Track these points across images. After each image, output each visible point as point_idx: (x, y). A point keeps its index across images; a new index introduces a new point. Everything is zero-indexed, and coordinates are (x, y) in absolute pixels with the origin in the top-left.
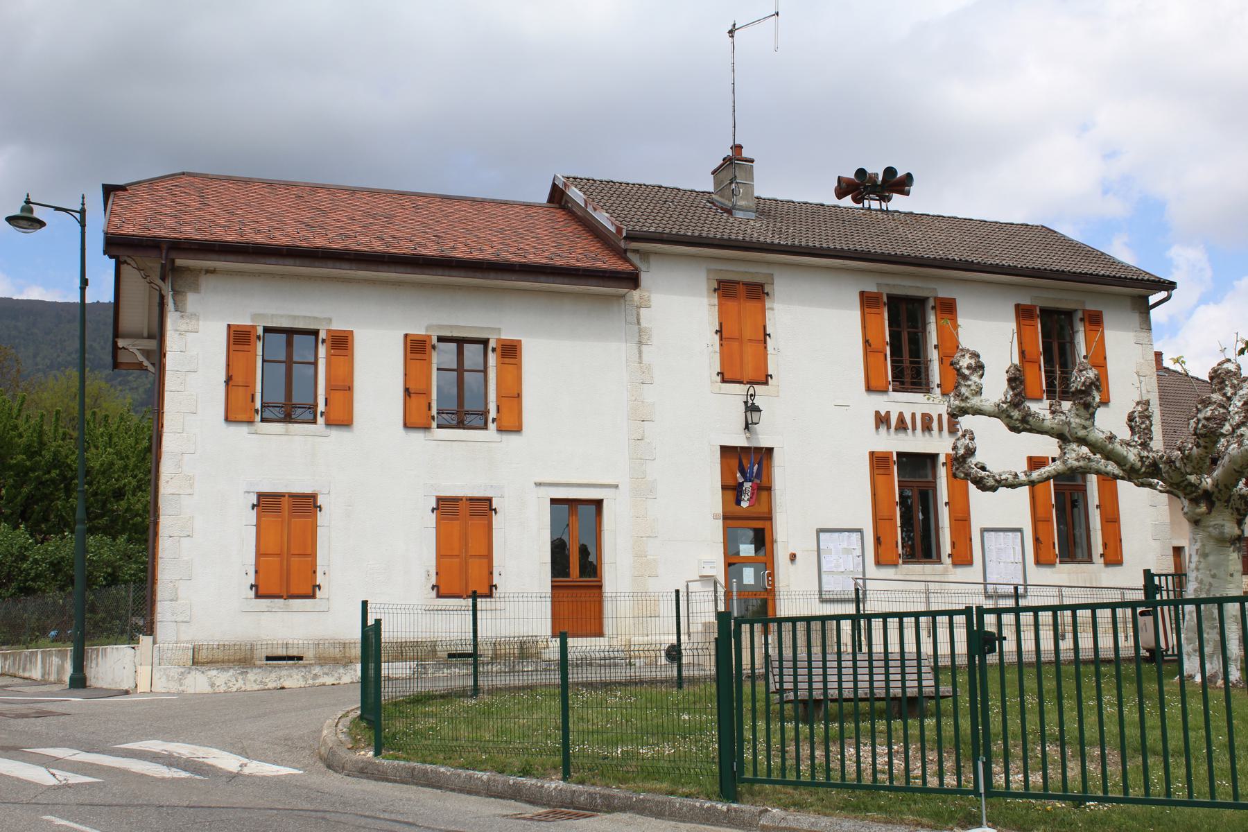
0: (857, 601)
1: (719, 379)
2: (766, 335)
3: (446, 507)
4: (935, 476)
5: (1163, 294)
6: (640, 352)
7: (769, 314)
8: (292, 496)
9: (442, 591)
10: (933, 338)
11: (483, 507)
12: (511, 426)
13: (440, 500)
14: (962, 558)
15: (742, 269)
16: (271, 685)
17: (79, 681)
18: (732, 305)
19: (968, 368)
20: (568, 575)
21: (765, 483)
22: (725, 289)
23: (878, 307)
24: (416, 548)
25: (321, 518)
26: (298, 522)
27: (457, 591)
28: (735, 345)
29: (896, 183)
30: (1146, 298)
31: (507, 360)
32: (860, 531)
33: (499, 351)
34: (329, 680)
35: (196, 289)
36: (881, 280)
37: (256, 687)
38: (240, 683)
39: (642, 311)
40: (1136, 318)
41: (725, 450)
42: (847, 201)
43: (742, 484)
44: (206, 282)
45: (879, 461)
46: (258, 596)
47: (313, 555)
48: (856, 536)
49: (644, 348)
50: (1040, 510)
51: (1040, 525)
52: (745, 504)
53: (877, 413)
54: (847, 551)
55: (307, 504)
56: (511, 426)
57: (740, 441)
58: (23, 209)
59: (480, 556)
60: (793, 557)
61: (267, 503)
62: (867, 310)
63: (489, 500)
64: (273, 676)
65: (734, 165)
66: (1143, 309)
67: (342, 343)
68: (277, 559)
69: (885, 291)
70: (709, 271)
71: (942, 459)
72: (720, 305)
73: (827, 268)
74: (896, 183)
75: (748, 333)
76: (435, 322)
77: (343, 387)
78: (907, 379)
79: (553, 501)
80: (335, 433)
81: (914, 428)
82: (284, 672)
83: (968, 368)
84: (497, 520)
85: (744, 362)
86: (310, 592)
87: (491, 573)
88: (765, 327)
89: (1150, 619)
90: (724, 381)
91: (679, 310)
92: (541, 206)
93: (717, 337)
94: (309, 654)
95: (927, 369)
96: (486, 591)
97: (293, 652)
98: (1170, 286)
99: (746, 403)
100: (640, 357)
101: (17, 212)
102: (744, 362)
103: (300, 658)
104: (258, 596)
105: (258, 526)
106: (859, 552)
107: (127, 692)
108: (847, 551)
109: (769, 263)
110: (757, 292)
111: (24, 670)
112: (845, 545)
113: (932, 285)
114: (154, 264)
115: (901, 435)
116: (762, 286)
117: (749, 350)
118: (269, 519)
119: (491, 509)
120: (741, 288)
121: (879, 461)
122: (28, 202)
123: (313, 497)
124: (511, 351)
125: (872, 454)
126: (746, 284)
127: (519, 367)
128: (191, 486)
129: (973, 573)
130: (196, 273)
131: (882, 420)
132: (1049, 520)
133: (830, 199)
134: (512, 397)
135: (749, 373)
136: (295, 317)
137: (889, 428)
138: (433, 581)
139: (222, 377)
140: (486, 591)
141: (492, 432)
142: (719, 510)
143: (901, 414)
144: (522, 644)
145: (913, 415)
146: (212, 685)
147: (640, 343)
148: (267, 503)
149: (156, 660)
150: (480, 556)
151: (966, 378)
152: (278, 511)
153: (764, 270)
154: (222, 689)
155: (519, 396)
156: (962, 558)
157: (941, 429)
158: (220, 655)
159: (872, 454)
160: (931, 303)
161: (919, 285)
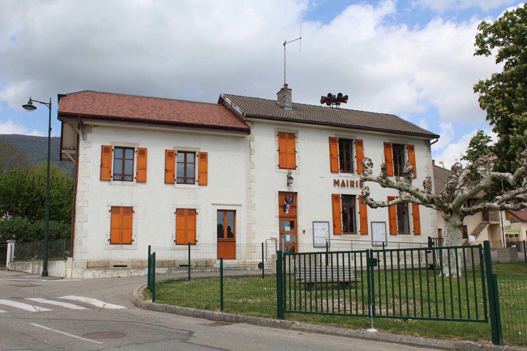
0: (384, 246)
1: (278, 167)
2: (295, 152)
3: (180, 212)
4: (355, 203)
5: (435, 140)
6: (250, 157)
7: (296, 144)
8: (124, 207)
9: (178, 243)
10: (355, 154)
11: (193, 212)
12: (204, 183)
13: (177, 209)
14: (364, 232)
15: (287, 128)
16: (115, 276)
17: (45, 274)
18: (283, 141)
19: (367, 164)
20: (223, 237)
21: (294, 205)
22: (281, 135)
23: (335, 142)
24: (168, 227)
25: (134, 216)
26: (126, 217)
27: (183, 243)
28: (284, 155)
29: (342, 99)
30: (429, 141)
31: (202, 160)
32: (328, 222)
33: (199, 156)
34: (136, 274)
35: (90, 132)
37: (110, 277)
38: (104, 275)
40: (426, 148)
41: (280, 193)
42: (325, 105)
43: (286, 205)
44: (94, 130)
45: (335, 197)
46: (111, 243)
48: (326, 224)
49: (252, 156)
50: (392, 215)
51: (392, 220)
52: (287, 212)
53: (335, 180)
54: (323, 229)
55: (129, 211)
56: (204, 183)
57: (285, 189)
58: (29, 103)
59: (192, 230)
60: (304, 231)
61: (114, 210)
63: (195, 210)
64: (116, 272)
65: (285, 91)
66: (429, 145)
67: (143, 152)
68: (118, 230)
69: (338, 137)
70: (275, 129)
71: (357, 197)
73: (317, 128)
74: (342, 99)
75: (289, 151)
76: (177, 146)
77: (143, 169)
79: (218, 210)
80: (140, 185)
81: (348, 186)
82: (120, 271)
83: (367, 164)
84: (198, 217)
85: (287, 161)
86: (130, 242)
90: (280, 168)
91: (264, 142)
92: (215, 105)
93: (278, 152)
94: (129, 265)
95: (352, 165)
96: (193, 242)
97: (124, 264)
98: (437, 137)
99: (288, 176)
100: (250, 159)
101: (27, 104)
102: (287, 161)
103: (126, 266)
104: (111, 243)
105: (111, 218)
106: (327, 230)
107: (63, 278)
108: (323, 229)
109: (297, 126)
110: (293, 136)
111: (26, 269)
112: (322, 227)
113: (354, 135)
114: (76, 123)
115: (343, 188)
116: (294, 134)
117: (289, 157)
120: (287, 135)
121: (335, 197)
122: (30, 100)
123: (131, 208)
124: (204, 156)
125: (333, 195)
126: (288, 134)
127: (206, 162)
128: (87, 203)
129: (368, 238)
130: (90, 126)
131: (336, 183)
132: (395, 219)
133: (319, 104)
134: (204, 173)
135: (289, 166)
136: (126, 143)
137: (339, 185)
138: (175, 239)
139: (99, 164)
140: (193, 242)
141: (196, 185)
142: (278, 214)
143: (343, 181)
144: (206, 262)
145: (347, 181)
146: (94, 276)
147: (250, 154)
148: (114, 210)
149: (73, 267)
150: (192, 230)
151: (366, 168)
152: (119, 213)
154: (98, 277)
155: (206, 172)
156: (364, 232)
157: (357, 186)
158: (97, 265)
159: (333, 195)
160: (354, 141)
161: (350, 135)
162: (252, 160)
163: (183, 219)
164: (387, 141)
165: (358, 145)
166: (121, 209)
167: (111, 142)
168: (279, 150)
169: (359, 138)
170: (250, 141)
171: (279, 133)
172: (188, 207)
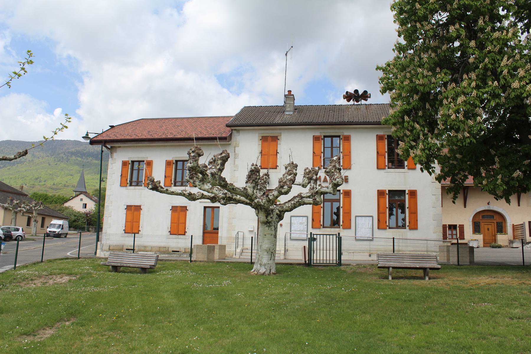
2: (277, 153)
6: (235, 161)
8: (135, 206)
13: (172, 207)
15: (270, 132)
18: (266, 144)
22: (264, 139)
24: (165, 220)
25: (142, 212)
27: (175, 233)
28: (266, 157)
35: (116, 152)
36: (321, 131)
44: (118, 150)
47: (139, 222)
48: (305, 219)
50: (381, 210)
51: (381, 215)
54: (301, 223)
55: (138, 208)
61: (129, 208)
63: (186, 207)
65: (289, 96)
67: (149, 164)
69: (323, 134)
72: (262, 144)
78: (396, 163)
84: (188, 213)
89: (245, 247)
100: (235, 162)
101: (85, 135)
106: (306, 224)
110: (275, 139)
112: (300, 221)
113: (341, 131)
116: (277, 137)
118: (129, 212)
123: (140, 206)
132: (385, 213)
133: (344, 102)
136: (139, 158)
153: (279, 131)
156: (348, 227)
158: (115, 248)
161: (337, 131)
162: (236, 163)
163: (176, 214)
164: (381, 133)
165: (344, 140)
166: (178, 208)
167: (129, 158)
168: (261, 153)
169: (346, 133)
170: (235, 147)
171: (262, 137)
172: (181, 205)
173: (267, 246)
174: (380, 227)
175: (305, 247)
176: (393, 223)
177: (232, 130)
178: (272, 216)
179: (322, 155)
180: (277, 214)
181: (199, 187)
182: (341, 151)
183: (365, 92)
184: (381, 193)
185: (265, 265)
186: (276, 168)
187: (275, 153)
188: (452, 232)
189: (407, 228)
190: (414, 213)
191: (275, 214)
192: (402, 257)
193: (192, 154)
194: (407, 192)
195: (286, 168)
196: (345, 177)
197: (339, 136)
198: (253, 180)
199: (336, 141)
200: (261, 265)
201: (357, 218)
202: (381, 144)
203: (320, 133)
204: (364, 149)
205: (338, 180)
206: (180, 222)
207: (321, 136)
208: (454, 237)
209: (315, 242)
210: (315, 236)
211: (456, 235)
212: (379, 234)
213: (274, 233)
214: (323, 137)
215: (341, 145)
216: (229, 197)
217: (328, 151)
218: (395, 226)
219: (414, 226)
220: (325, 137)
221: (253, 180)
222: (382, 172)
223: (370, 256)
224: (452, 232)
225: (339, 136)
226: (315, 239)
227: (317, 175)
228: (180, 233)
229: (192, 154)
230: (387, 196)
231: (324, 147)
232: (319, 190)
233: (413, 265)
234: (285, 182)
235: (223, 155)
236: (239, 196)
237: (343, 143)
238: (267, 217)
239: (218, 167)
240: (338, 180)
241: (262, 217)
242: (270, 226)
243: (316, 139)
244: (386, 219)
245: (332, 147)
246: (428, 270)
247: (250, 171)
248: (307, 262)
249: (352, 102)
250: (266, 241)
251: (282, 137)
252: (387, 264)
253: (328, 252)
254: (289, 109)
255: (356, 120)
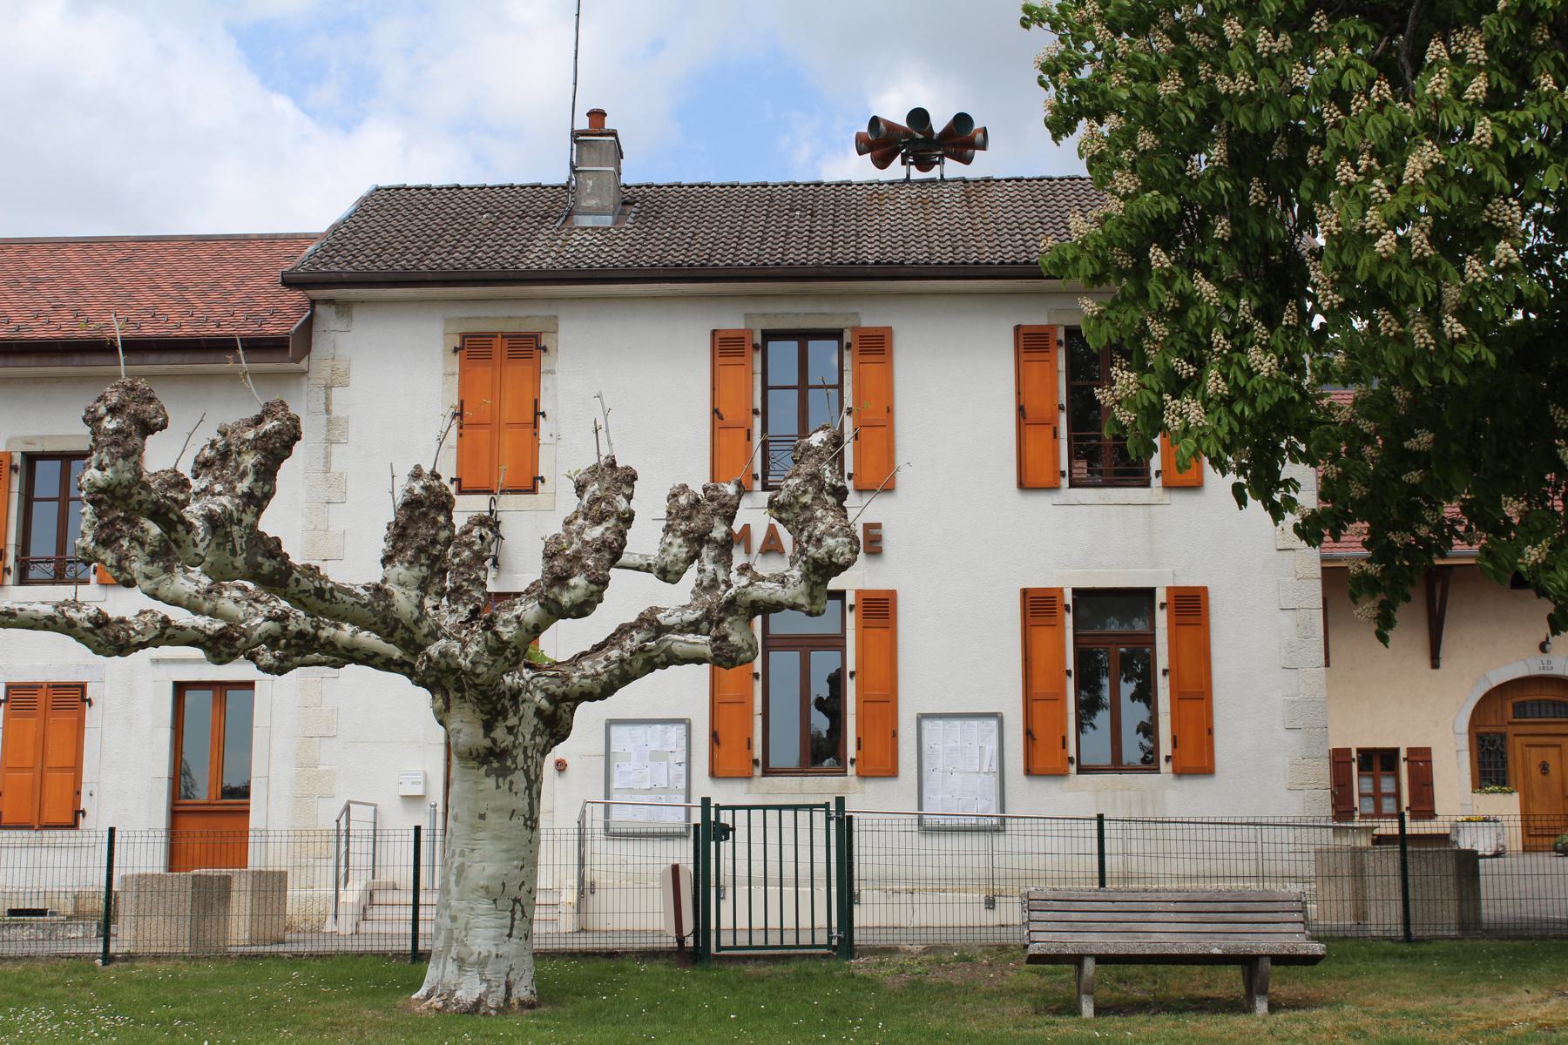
2: (538, 413)
6: (327, 457)
15: (500, 315)
18: (483, 372)
22: (472, 347)
27: (25, 819)
28: (483, 434)
32: (687, 723)
36: (754, 308)
39: (336, 393)
42: (896, 170)
48: (676, 732)
49: (335, 449)
51: (1038, 708)
54: (657, 756)
59: (62, 769)
62: (720, 360)
63: (82, 687)
65: (595, 137)
69: (759, 325)
70: (447, 321)
84: (91, 715)
87: (79, 793)
88: (536, 403)
89: (385, 876)
106: (682, 757)
109: (551, 300)
110: (528, 347)
112: (655, 746)
116: (536, 337)
117: (508, 439)
119: (84, 700)
132: (1059, 698)
133: (861, 169)
150: (62, 769)
161: (826, 308)
162: (337, 464)
163: (31, 725)
164: (1036, 318)
165: (863, 352)
166: (42, 694)
168: (459, 414)
169: (871, 318)
170: (328, 387)
171: (464, 336)
172: (54, 679)
173: (491, 869)
174: (1037, 766)
175: (675, 869)
176: (1097, 744)
177: (313, 303)
178: (513, 721)
179: (758, 421)
180: (539, 712)
181: (148, 585)
182: (848, 403)
183: (962, 121)
184: (1038, 605)
185: (482, 963)
186: (534, 491)
187: (530, 418)
188: (1377, 786)
189: (1165, 767)
190: (1196, 695)
191: (528, 710)
192: (1141, 906)
193: (110, 424)
194: (1161, 597)
195: (580, 488)
196: (867, 527)
197: (836, 334)
198: (421, 550)
199: (823, 354)
200: (461, 962)
201: (926, 724)
202: (1035, 370)
203: (747, 316)
204: (957, 393)
205: (830, 542)
206: (52, 761)
207: (751, 332)
208: (1388, 806)
209: (726, 846)
210: (726, 817)
211: (1397, 795)
212: (1030, 797)
213: (522, 804)
214: (758, 339)
215: (848, 378)
216: (301, 634)
217: (784, 409)
218: (1106, 760)
219: (1196, 760)
220: (768, 335)
221: (421, 550)
222: (1041, 502)
223: (990, 904)
224: (1377, 786)
225: (836, 334)
226: (724, 832)
227: (730, 519)
228: (50, 817)
229: (110, 424)
230: (1069, 618)
231: (765, 388)
232: (742, 592)
233: (1191, 946)
234: (577, 557)
235: (268, 426)
236: (347, 630)
237: (858, 365)
238: (488, 727)
239: (243, 487)
240: (830, 542)
241: (467, 729)
242: (503, 773)
243: (726, 346)
244: (1064, 727)
245: (803, 387)
246: (1266, 965)
247: (406, 505)
248: (690, 942)
249: (896, 171)
250: (487, 847)
251: (561, 335)
252: (1071, 942)
253: (789, 890)
254: (592, 202)
255: (917, 254)
